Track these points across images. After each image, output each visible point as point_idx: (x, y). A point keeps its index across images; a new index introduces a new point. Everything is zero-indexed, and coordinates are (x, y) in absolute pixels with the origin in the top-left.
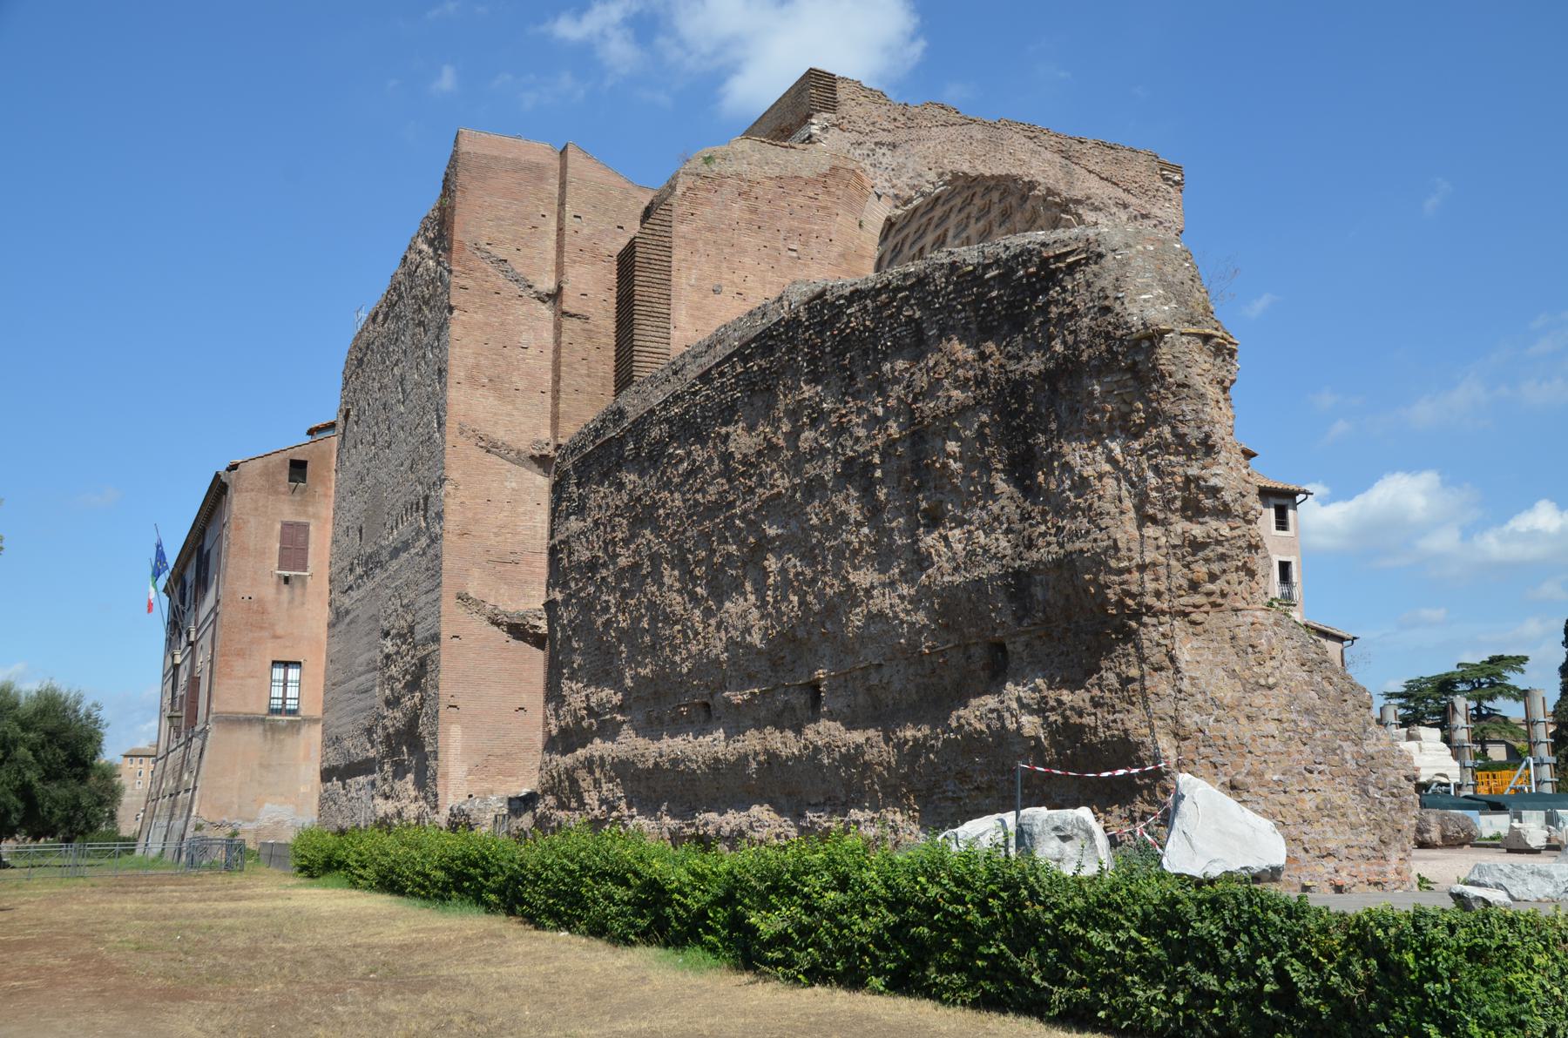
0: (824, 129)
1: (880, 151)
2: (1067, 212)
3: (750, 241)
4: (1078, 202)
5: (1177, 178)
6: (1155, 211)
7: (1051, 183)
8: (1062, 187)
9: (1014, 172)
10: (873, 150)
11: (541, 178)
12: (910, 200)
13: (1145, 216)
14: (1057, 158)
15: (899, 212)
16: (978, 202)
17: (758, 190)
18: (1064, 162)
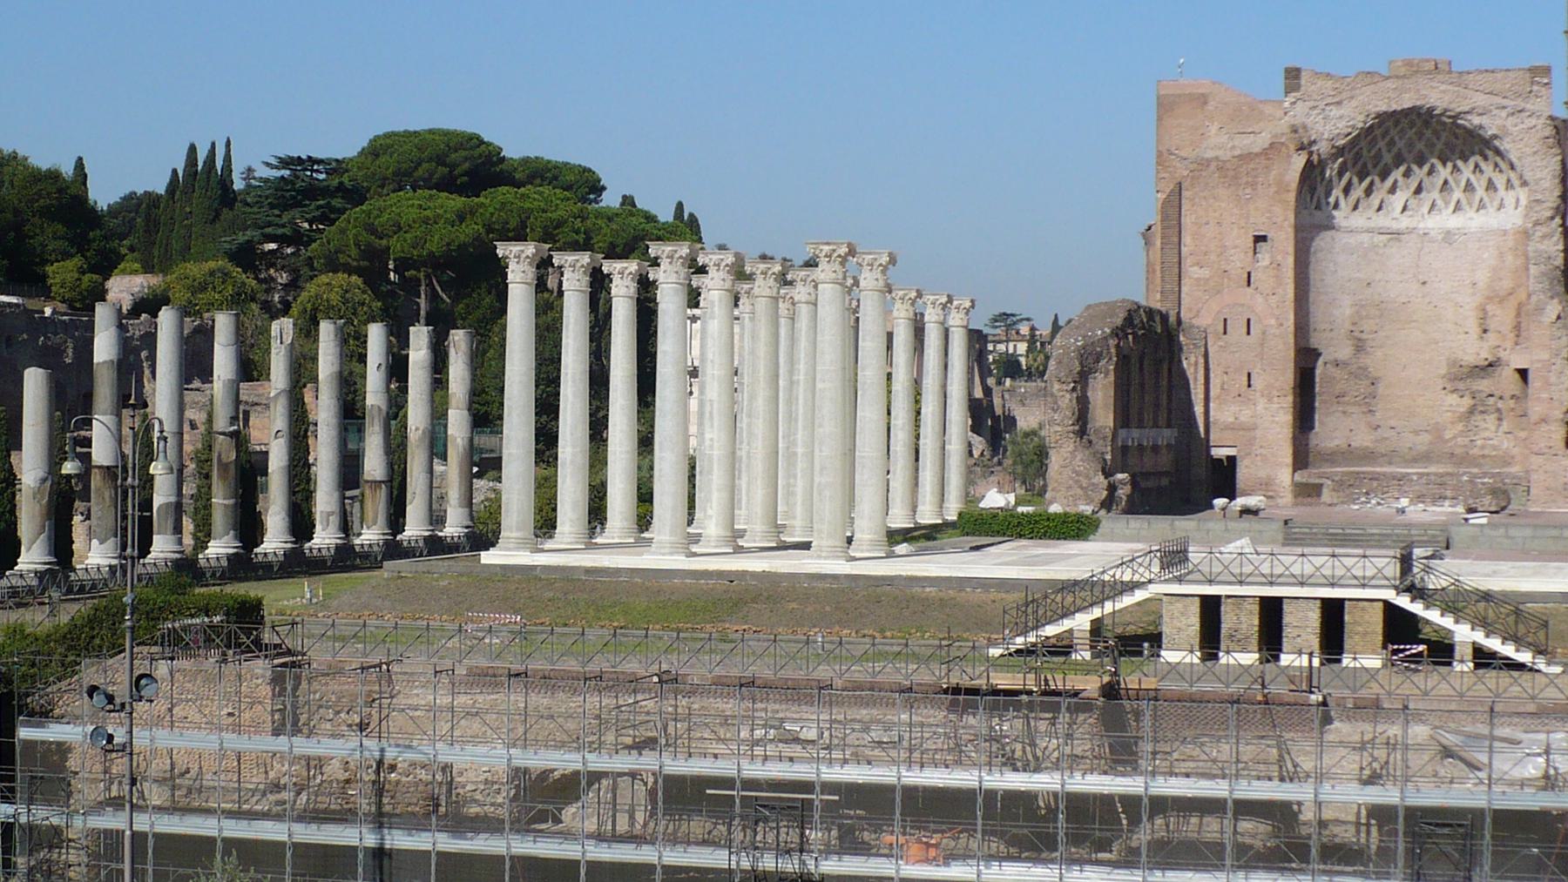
0: (1294, 103)
1: (1328, 108)
2: (1461, 119)
3: (1222, 192)
4: (1468, 112)
5: (1546, 81)
6: (1528, 106)
7: (1445, 105)
8: (1451, 107)
9: (1418, 103)
10: (1323, 110)
11: (1205, 103)
12: (1349, 134)
13: (1520, 111)
14: (1450, 87)
15: (1343, 142)
16: (1405, 122)
17: (1228, 165)
18: (1456, 89)
